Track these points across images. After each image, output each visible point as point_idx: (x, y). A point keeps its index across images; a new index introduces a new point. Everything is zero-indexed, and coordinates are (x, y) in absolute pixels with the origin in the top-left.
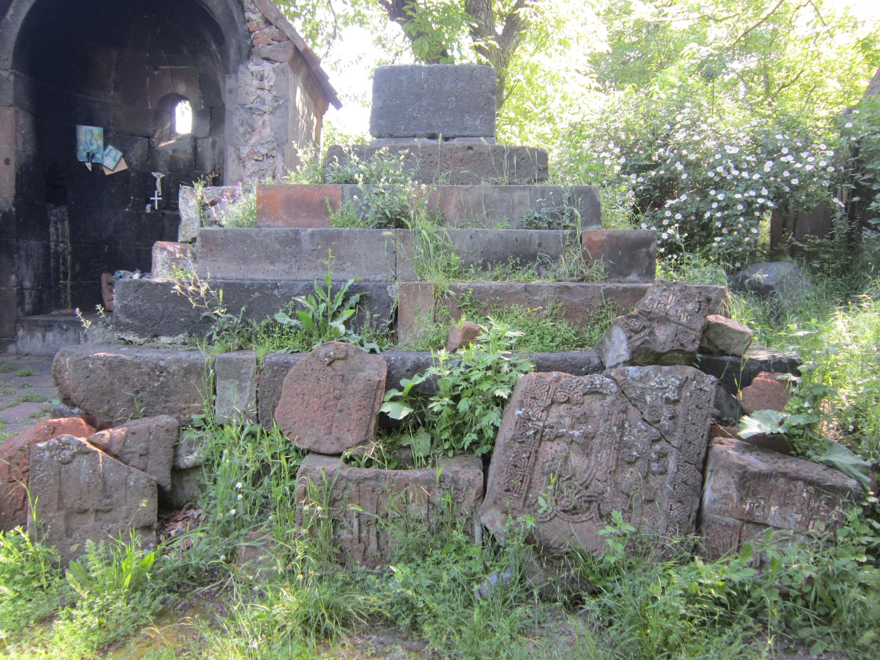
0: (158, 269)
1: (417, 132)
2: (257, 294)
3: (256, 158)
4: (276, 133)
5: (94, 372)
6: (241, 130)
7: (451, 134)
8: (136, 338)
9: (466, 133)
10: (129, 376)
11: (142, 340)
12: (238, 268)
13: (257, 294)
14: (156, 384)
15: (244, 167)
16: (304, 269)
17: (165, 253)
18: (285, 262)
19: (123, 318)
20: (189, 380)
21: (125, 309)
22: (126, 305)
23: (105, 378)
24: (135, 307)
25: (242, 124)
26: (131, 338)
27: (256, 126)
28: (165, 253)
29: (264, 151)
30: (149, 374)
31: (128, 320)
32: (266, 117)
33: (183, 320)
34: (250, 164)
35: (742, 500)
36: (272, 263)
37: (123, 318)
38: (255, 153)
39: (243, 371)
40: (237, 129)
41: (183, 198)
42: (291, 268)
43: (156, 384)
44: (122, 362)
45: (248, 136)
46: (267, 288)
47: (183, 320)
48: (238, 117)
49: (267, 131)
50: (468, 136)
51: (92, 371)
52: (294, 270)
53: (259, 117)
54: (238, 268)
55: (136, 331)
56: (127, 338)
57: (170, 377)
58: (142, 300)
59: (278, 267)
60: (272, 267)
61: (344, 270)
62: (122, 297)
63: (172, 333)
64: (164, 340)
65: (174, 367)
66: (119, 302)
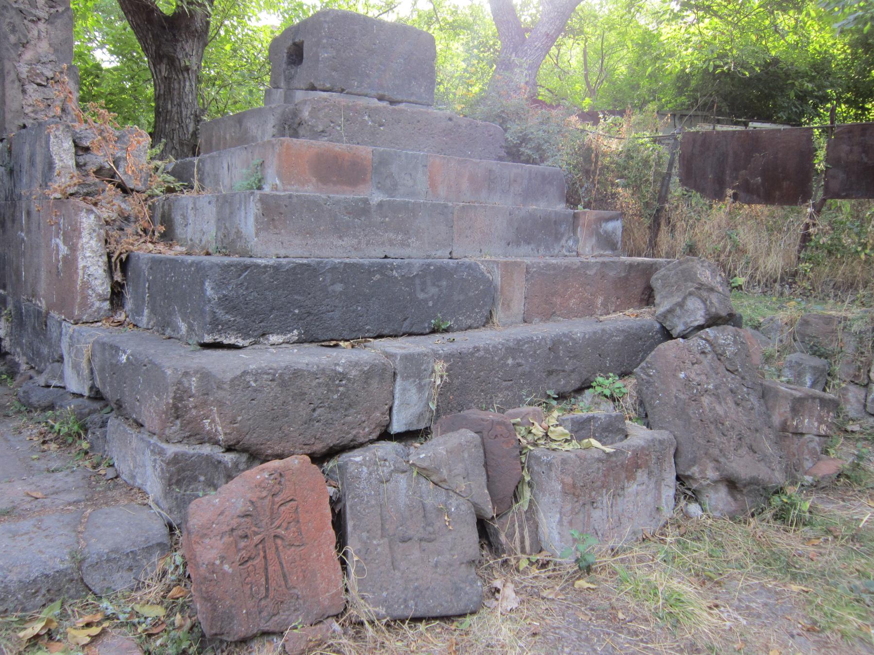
0: (84, 240)
1: (369, 91)
2: (378, 276)
3: (39, 81)
4: (56, 51)
5: (260, 391)
6: (13, 39)
7: (399, 98)
8: (239, 340)
9: (412, 99)
10: (305, 390)
11: (246, 343)
12: (304, 243)
13: (378, 276)
14: (336, 397)
15: (24, 92)
16: (372, 243)
17: (92, 217)
18: (355, 236)
19: (221, 314)
20: (369, 385)
21: (224, 301)
22: (225, 296)
23: (276, 397)
24: (238, 297)
25: (14, 30)
26: (232, 341)
27: (30, 36)
28: (92, 217)
29: (50, 74)
30: (327, 385)
31: (228, 317)
32: (42, 26)
33: (297, 311)
34: (31, 88)
35: (793, 419)
36: (340, 237)
37: (221, 314)
38: (37, 75)
39: (423, 368)
40: (6, 38)
41: (56, 137)
42: (359, 243)
43: (336, 397)
44: (297, 374)
45: (21, 49)
46: (387, 269)
47: (297, 311)
48: (8, 20)
49: (44, 47)
50: (412, 103)
51: (255, 390)
52: (363, 246)
53: (31, 25)
54: (304, 243)
55: (239, 330)
56: (226, 342)
57: (350, 385)
58: (247, 289)
59: (347, 242)
60: (341, 242)
61: (409, 246)
62: (219, 285)
63: (282, 331)
64: (274, 338)
65: (354, 373)
66: (217, 293)
